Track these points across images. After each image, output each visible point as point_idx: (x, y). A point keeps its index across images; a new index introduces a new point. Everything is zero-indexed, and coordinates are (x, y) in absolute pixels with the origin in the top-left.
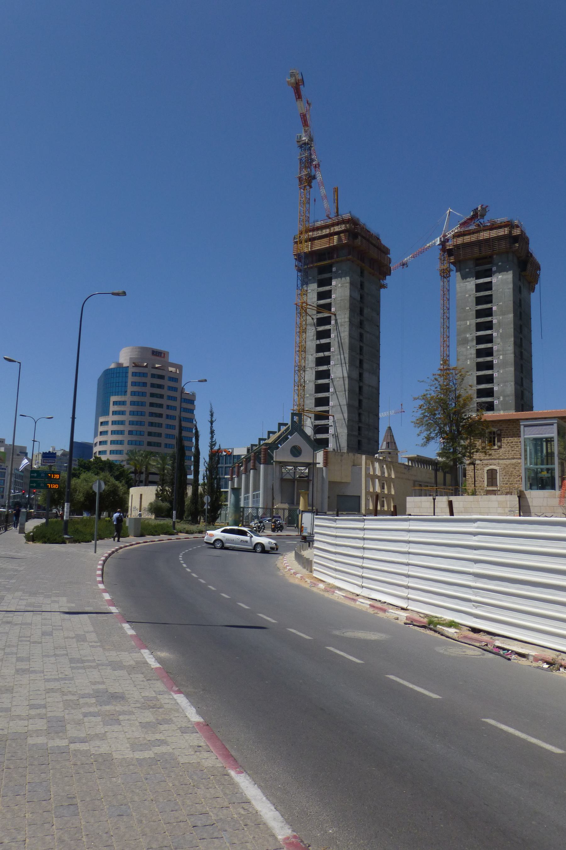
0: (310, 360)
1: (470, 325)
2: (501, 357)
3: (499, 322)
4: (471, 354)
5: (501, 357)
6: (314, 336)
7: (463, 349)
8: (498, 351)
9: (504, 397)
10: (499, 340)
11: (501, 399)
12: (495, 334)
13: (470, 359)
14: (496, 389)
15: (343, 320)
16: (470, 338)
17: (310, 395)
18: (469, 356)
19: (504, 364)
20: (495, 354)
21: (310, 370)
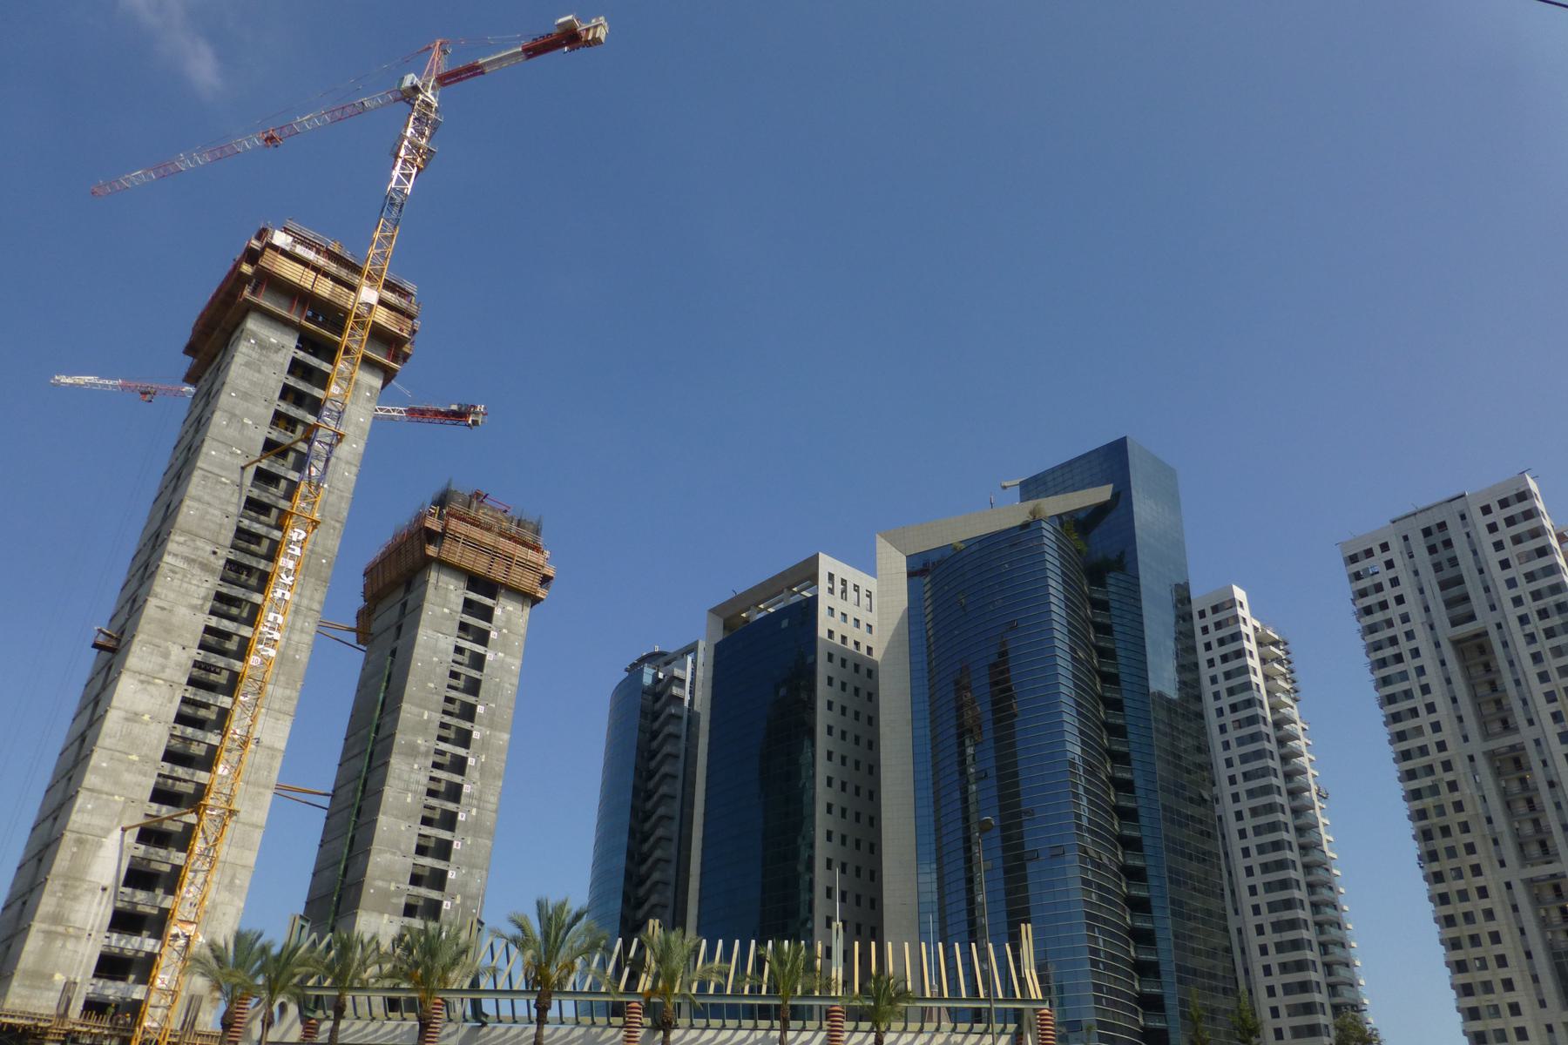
0: (173, 658)
1: (429, 720)
2: (474, 812)
3: (483, 738)
4: (418, 783)
5: (474, 812)
6: (205, 599)
7: (405, 768)
8: (470, 796)
9: (464, 898)
10: (476, 775)
11: (458, 900)
12: (471, 761)
13: (415, 792)
14: (451, 875)
15: (305, 602)
16: (423, 749)
17: (144, 759)
18: (413, 787)
19: (476, 828)
20: (463, 800)
21: (165, 688)
